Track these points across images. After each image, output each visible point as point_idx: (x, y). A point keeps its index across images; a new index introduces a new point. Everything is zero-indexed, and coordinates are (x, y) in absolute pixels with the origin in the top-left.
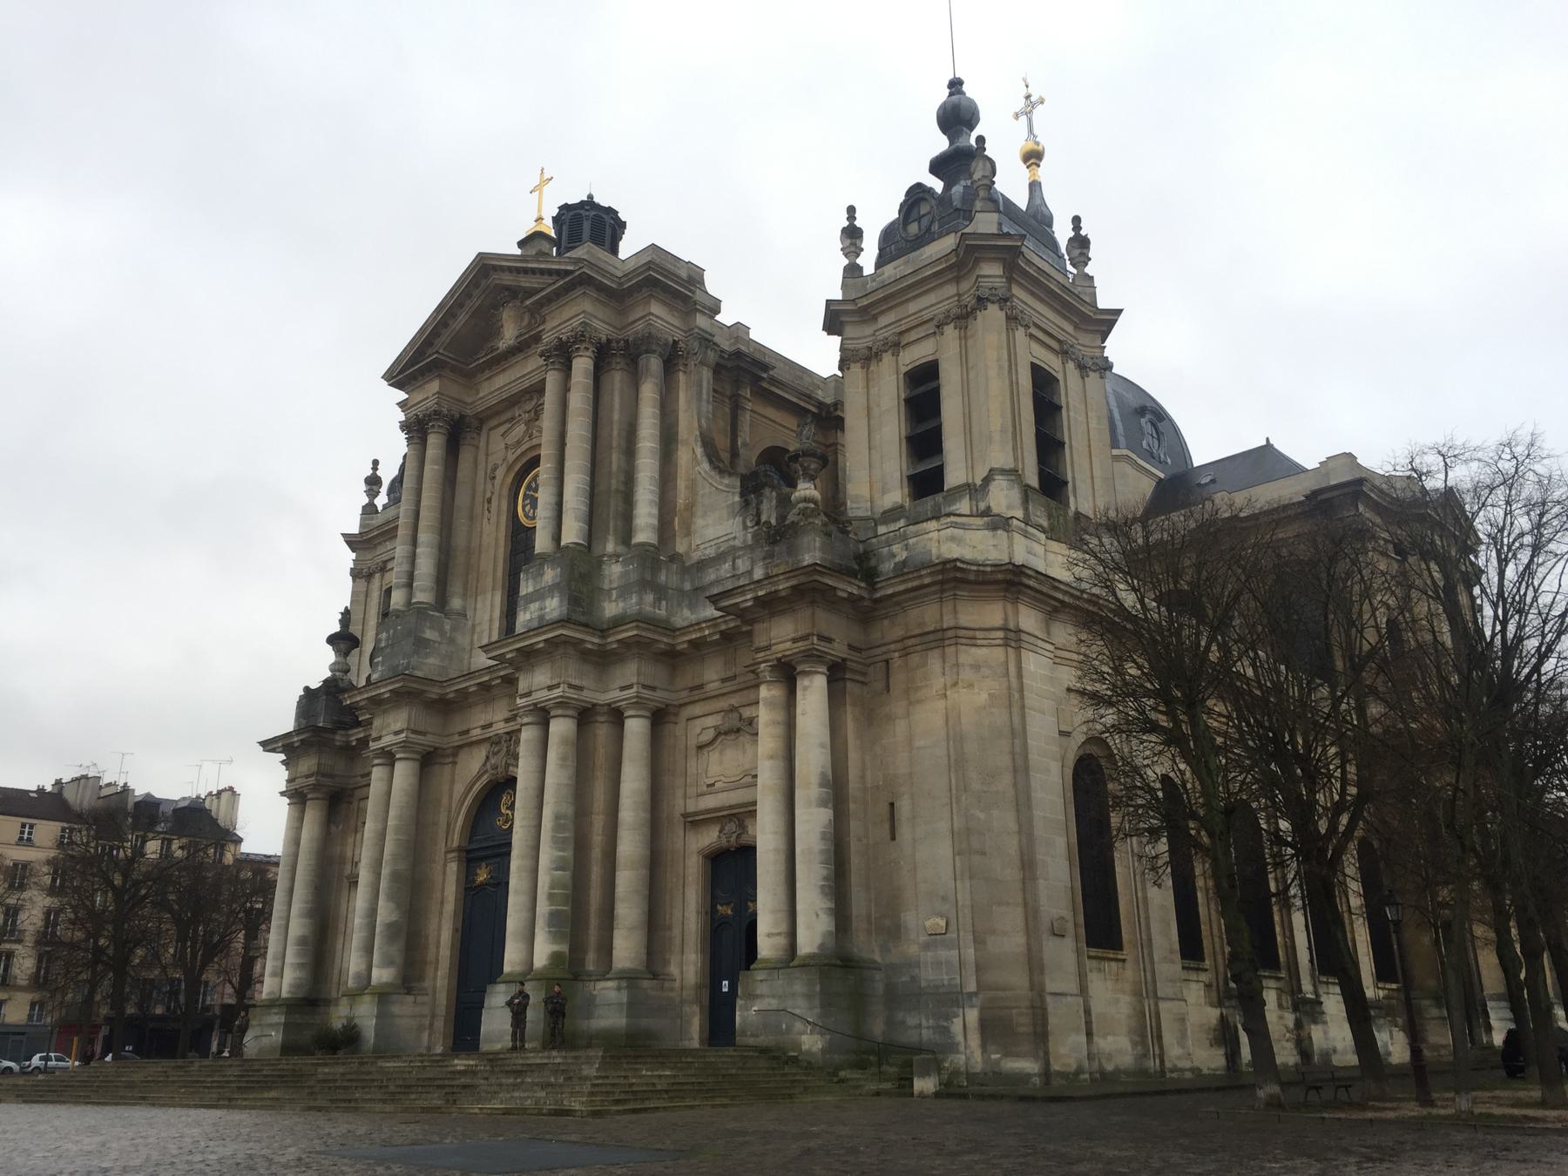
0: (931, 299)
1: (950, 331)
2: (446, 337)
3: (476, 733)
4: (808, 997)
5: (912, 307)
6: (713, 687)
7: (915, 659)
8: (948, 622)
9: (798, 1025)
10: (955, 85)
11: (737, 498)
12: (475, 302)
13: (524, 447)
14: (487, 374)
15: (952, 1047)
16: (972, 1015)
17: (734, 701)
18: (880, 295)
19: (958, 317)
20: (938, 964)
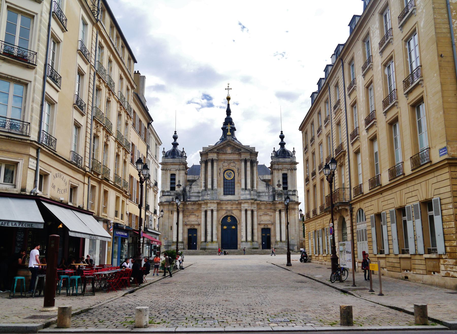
0: (287, 166)
1: (289, 170)
2: (218, 148)
3: (224, 208)
4: (286, 245)
5: (284, 166)
6: (263, 209)
7: (290, 211)
8: (294, 207)
9: (284, 247)
10: (282, 132)
11: (265, 185)
12: (225, 145)
13: (227, 167)
14: (222, 154)
15: (294, 250)
16: (296, 247)
17: (266, 211)
18: (281, 163)
19: (291, 170)
20: (293, 242)
